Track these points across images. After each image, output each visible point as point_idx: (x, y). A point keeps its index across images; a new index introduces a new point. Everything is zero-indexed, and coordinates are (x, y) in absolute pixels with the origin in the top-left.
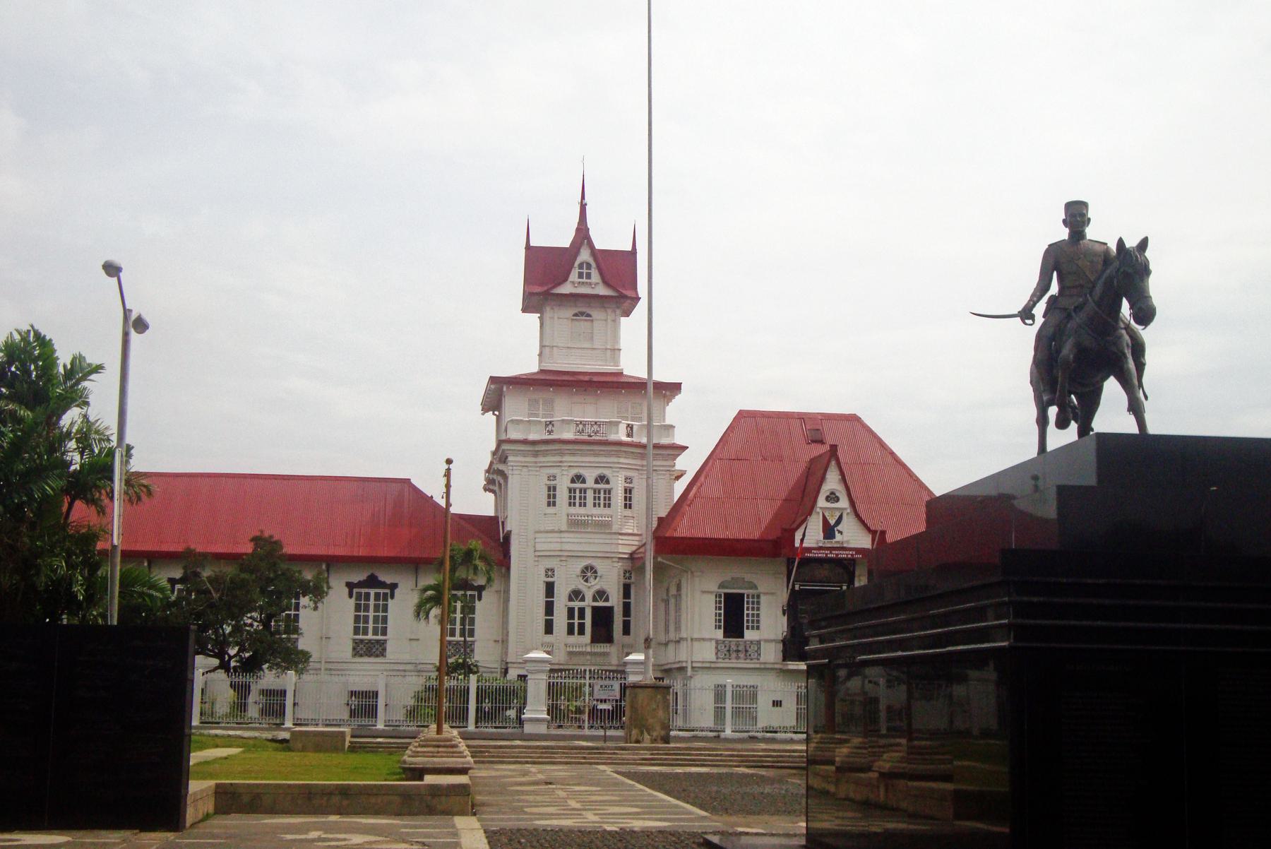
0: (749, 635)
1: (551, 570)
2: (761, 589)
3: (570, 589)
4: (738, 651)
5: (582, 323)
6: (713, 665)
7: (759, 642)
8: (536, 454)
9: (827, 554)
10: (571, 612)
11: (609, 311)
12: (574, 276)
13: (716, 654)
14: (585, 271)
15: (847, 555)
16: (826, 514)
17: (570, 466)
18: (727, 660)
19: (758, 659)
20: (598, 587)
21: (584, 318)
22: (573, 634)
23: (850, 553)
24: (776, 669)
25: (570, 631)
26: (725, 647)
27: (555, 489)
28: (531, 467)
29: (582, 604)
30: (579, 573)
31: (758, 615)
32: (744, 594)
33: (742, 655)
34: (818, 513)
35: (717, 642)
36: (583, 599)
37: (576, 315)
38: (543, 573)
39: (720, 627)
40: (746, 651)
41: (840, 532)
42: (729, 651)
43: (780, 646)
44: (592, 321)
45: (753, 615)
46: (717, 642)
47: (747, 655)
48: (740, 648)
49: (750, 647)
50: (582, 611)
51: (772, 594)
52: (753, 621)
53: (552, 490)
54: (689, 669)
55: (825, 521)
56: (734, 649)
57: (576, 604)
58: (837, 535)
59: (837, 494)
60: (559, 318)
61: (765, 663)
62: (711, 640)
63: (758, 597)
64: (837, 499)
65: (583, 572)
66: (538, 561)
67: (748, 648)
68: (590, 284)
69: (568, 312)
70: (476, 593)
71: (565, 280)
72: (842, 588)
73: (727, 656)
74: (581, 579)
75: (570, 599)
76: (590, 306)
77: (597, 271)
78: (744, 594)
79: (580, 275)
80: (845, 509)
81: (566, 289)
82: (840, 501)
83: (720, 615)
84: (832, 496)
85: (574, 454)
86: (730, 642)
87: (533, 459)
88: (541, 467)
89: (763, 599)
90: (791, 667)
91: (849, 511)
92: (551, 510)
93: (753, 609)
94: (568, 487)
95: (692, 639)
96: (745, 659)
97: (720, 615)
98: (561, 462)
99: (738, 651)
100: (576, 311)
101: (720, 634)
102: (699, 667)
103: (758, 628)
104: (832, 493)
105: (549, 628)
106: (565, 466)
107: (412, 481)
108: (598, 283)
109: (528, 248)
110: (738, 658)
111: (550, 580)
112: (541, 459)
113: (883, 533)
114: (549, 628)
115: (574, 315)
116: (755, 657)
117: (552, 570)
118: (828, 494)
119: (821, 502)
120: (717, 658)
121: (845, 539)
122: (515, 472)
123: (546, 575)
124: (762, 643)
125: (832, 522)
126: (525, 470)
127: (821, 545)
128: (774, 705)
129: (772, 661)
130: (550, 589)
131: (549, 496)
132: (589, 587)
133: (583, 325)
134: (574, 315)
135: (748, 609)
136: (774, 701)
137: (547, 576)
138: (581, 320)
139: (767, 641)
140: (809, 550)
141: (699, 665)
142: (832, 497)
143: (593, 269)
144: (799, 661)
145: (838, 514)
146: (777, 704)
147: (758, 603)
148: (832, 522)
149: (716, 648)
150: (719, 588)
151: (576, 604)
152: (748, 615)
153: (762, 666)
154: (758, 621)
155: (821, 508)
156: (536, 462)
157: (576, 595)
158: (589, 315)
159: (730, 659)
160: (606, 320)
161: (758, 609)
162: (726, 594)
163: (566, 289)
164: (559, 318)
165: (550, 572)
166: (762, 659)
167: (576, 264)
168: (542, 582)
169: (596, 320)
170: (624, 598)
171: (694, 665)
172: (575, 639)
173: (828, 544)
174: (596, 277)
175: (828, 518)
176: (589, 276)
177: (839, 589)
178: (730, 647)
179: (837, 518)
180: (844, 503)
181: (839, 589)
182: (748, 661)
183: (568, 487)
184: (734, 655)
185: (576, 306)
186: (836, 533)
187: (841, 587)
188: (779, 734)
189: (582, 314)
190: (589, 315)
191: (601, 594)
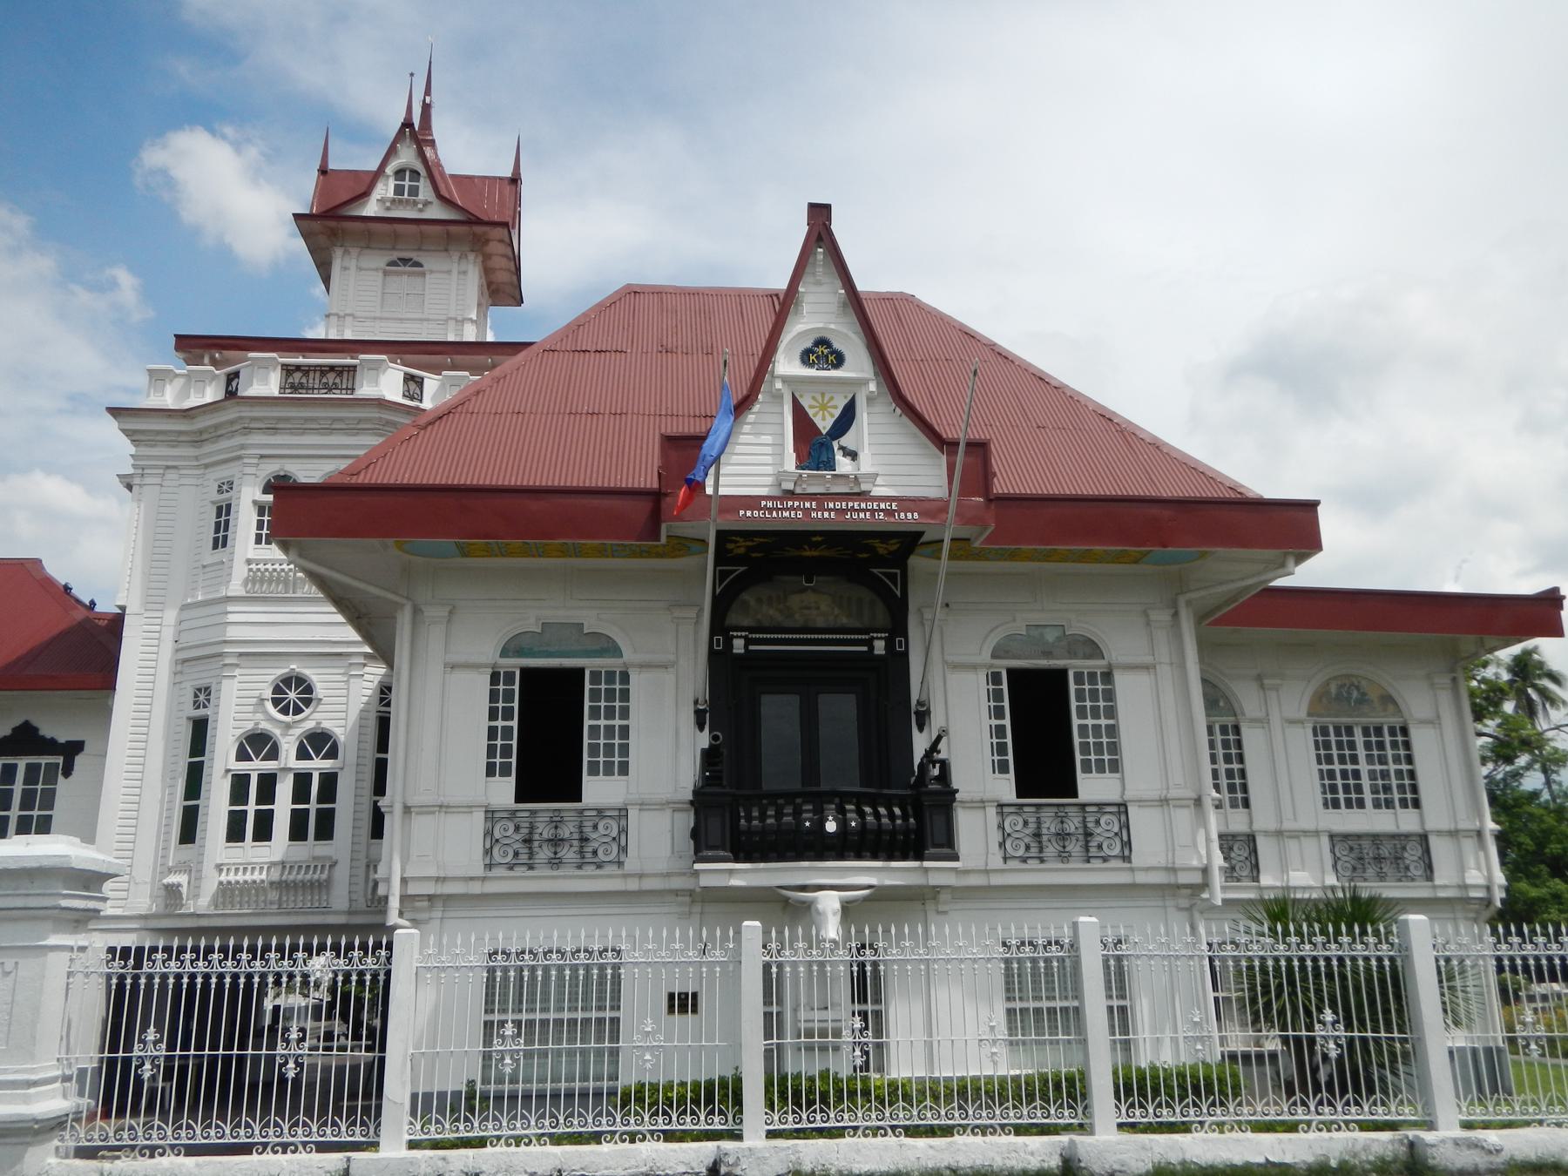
0: (597, 790)
1: (206, 689)
2: (628, 655)
3: (242, 731)
4: (556, 842)
5: (405, 277)
6: (476, 888)
7: (622, 813)
8: (198, 439)
9: (807, 511)
10: (239, 785)
11: (456, 256)
12: (385, 189)
13: (488, 852)
14: (407, 183)
15: (873, 511)
16: (805, 402)
17: (262, 457)
18: (520, 871)
19: (620, 864)
20: (309, 725)
21: (408, 269)
22: (242, 840)
23: (882, 506)
24: (676, 893)
25: (235, 832)
26: (517, 828)
27: (229, 507)
28: (185, 467)
29: (270, 766)
30: (268, 694)
31: (625, 732)
32: (580, 672)
33: (568, 854)
34: (778, 397)
35: (491, 815)
36: (273, 754)
38: (190, 698)
39: (505, 771)
40: (584, 840)
41: (853, 455)
42: (528, 841)
43: (687, 820)
44: (423, 274)
45: (610, 731)
46: (491, 815)
47: (587, 856)
48: (566, 831)
49: (595, 827)
50: (268, 785)
51: (664, 666)
52: (609, 749)
53: (224, 513)
54: (394, 903)
55: (803, 422)
56: (545, 836)
57: (256, 767)
58: (844, 465)
59: (837, 345)
60: (360, 269)
61: (641, 876)
62: (469, 808)
63: (625, 678)
64: (838, 360)
65: (277, 689)
66: (181, 672)
67: (588, 830)
69: (378, 260)
70: (60, 760)
71: (366, 194)
72: (872, 648)
73: (524, 858)
74: (269, 706)
75: (242, 755)
76: (419, 249)
77: (428, 183)
78: (581, 671)
79: (399, 190)
80: (865, 382)
81: (371, 208)
82: (846, 364)
83: (507, 732)
84: (820, 350)
85: (274, 430)
86: (533, 812)
87: (190, 451)
88: (206, 466)
89: (637, 681)
90: (705, 881)
91: (872, 387)
92: (221, 554)
93: (610, 713)
94: (255, 502)
95: (407, 810)
96: (580, 867)
97: (507, 732)
98: (243, 447)
99: (556, 842)
100: (395, 255)
101: (503, 791)
102: (430, 898)
103: (624, 769)
104: (822, 342)
105: (189, 832)
106: (250, 456)
107: (43, 562)
108: (431, 203)
109: (323, 171)
110: (555, 862)
111: (201, 712)
112: (208, 448)
113: (979, 448)
114: (189, 832)
115: (389, 264)
116: (611, 858)
117: (207, 690)
118: (809, 344)
119: (787, 365)
120: (489, 866)
121: (866, 464)
122: (148, 480)
123: (195, 702)
124: (633, 814)
125: (824, 423)
126: (171, 475)
127: (789, 486)
128: (671, 1010)
129: (662, 867)
130: (200, 732)
131: (218, 525)
132: (288, 726)
133: (403, 282)
134: (388, 265)
135: (595, 713)
136: (671, 996)
137: (197, 705)
138: (404, 273)
139: (643, 806)
140: (752, 502)
141: (429, 889)
142: (822, 352)
143: (422, 180)
144: (737, 860)
145: (840, 403)
146: (683, 1003)
147: (625, 695)
148: (824, 423)
149: (489, 833)
150: (504, 653)
151: (256, 767)
152: (594, 730)
153: (633, 885)
154: (625, 750)
155: (786, 380)
156: (197, 458)
157: (258, 743)
158: (419, 265)
159: (531, 867)
160: (449, 272)
161: (625, 713)
162: (525, 672)
163: (371, 208)
165: (203, 695)
166: (631, 864)
167: (389, 170)
168: (184, 721)
169: (432, 272)
170: (379, 751)
171: (413, 889)
172: (249, 850)
173: (816, 483)
174: (425, 191)
175: (811, 412)
176: (414, 191)
177: (865, 649)
178: (532, 828)
179: (837, 413)
180: (858, 366)
181: (865, 649)
182: (589, 870)
183: (255, 502)
184: (544, 853)
185: (394, 249)
186: (839, 457)
187: (869, 642)
188: (605, 1147)
189: (405, 261)
190: (419, 265)
191: (319, 742)
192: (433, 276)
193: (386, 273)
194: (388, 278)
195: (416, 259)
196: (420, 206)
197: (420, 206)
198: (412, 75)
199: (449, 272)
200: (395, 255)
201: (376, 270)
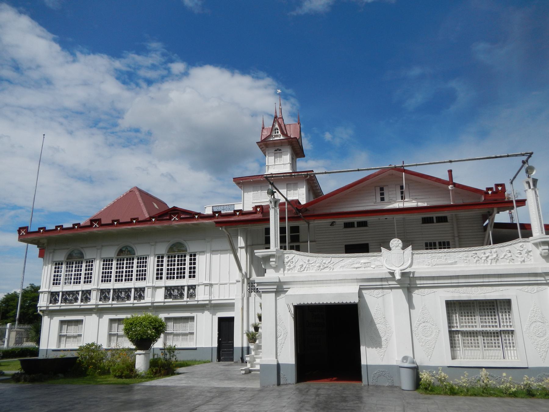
5: (278, 154)
37: (276, 150)
44: (281, 153)
60: (269, 153)
68: (278, 135)
69: (273, 151)
76: (281, 146)
100: (276, 148)
164: (269, 153)
169: (284, 152)
176: (278, 132)
185: (275, 147)
190: (280, 150)
192: (285, 152)
193: (275, 153)
194: (275, 155)
195: (280, 149)
196: (279, 136)
197: (279, 136)
198: (275, 103)
199: (288, 151)
200: (276, 148)
201: (273, 153)
